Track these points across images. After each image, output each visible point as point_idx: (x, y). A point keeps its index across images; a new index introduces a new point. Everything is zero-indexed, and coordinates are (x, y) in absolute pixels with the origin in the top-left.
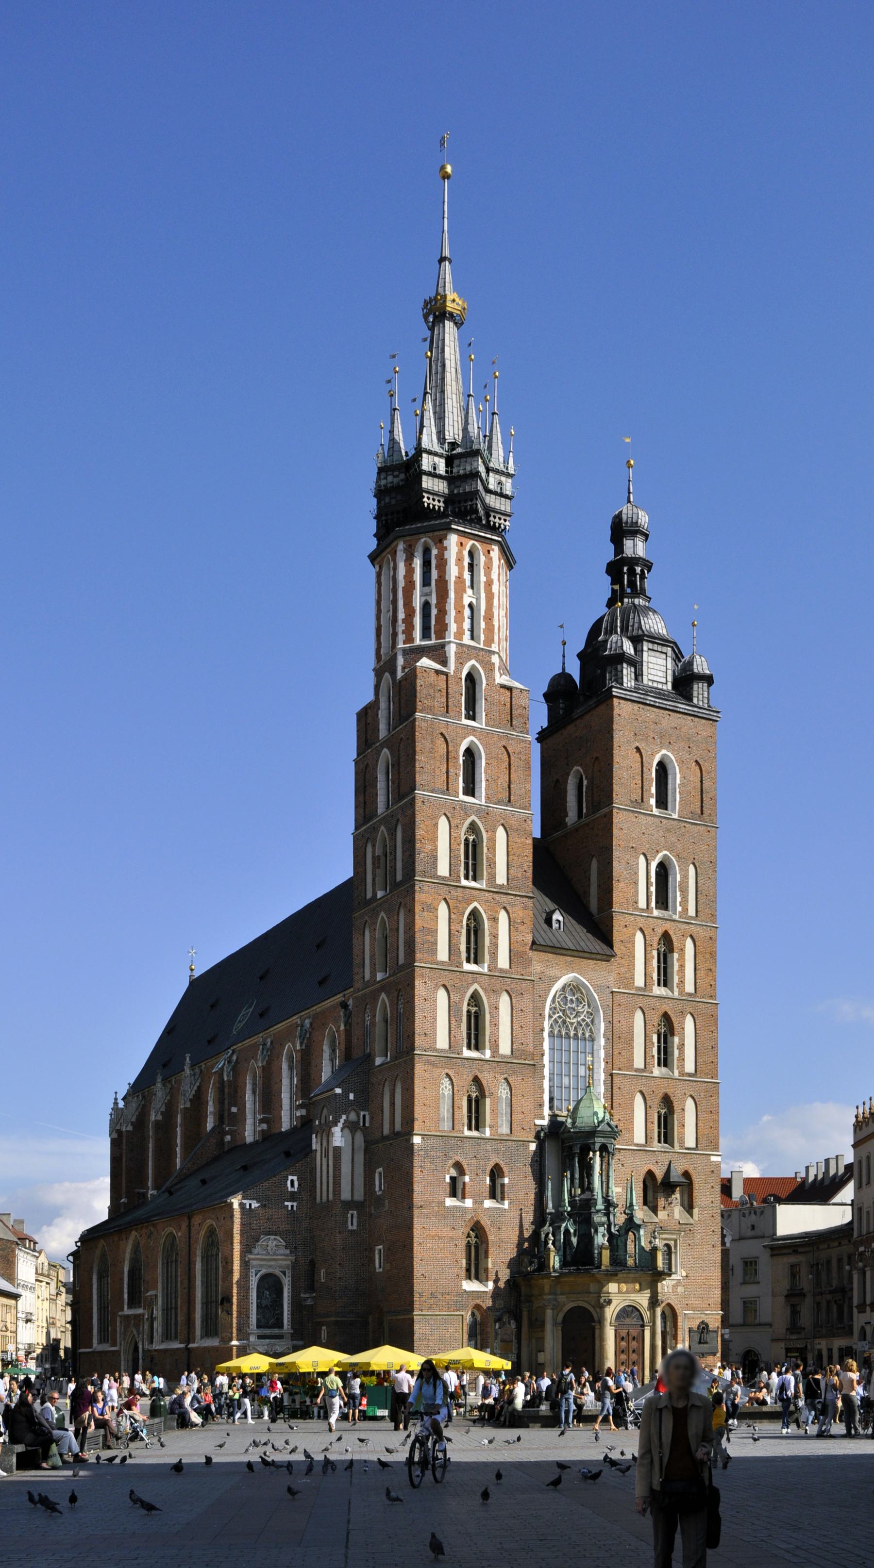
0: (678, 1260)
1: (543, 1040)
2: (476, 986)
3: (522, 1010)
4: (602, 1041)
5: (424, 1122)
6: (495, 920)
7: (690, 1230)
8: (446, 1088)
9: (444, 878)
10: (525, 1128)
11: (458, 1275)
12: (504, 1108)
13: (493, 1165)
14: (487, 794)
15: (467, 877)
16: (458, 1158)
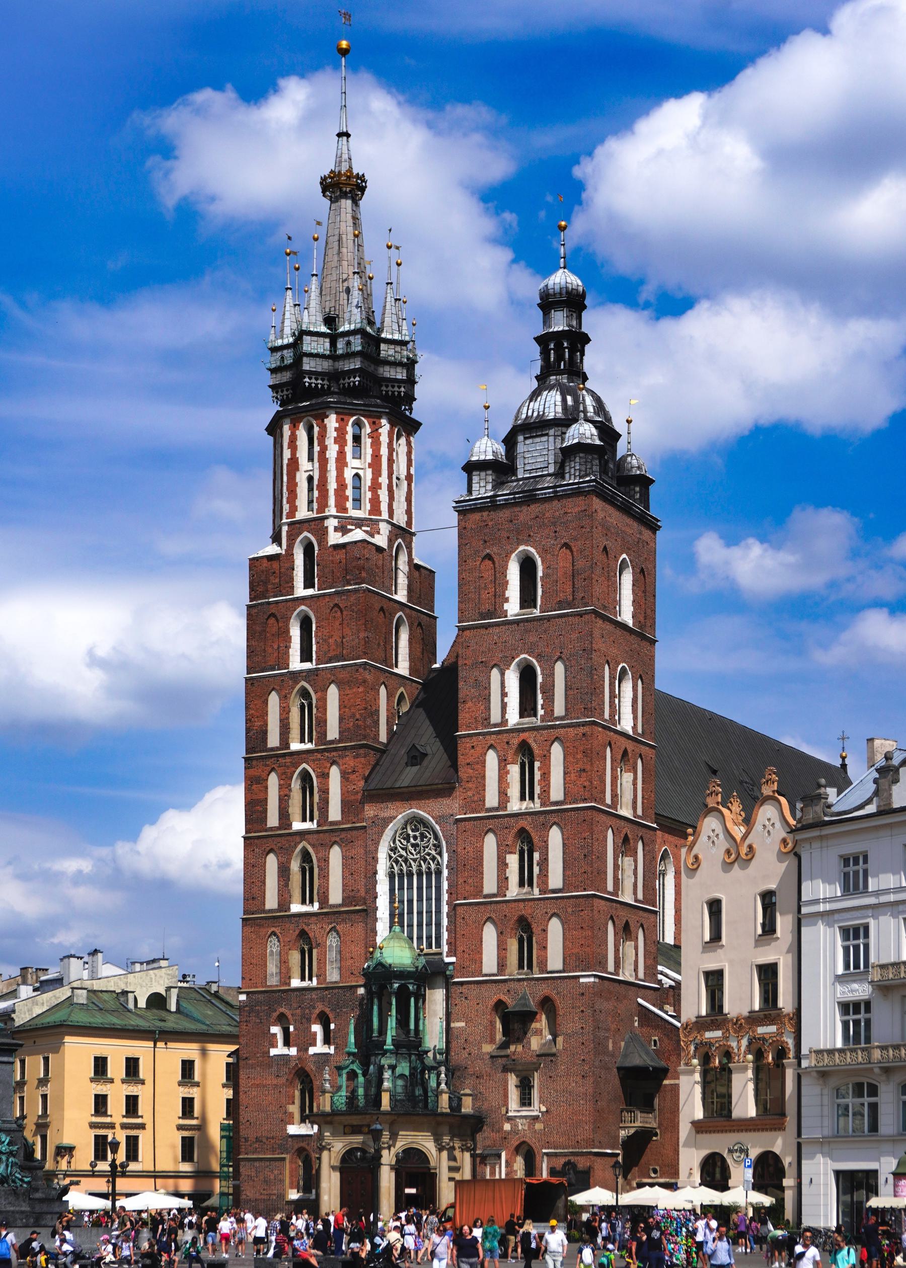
0: (535, 1094)
1: (376, 882)
2: (304, 843)
3: (352, 858)
4: (445, 873)
5: (250, 980)
6: (325, 776)
7: (552, 1061)
8: (275, 944)
9: (272, 749)
10: (355, 973)
11: (282, 1121)
12: (332, 955)
13: (318, 1012)
14: (317, 657)
15: (302, 741)
16: (282, 1010)
